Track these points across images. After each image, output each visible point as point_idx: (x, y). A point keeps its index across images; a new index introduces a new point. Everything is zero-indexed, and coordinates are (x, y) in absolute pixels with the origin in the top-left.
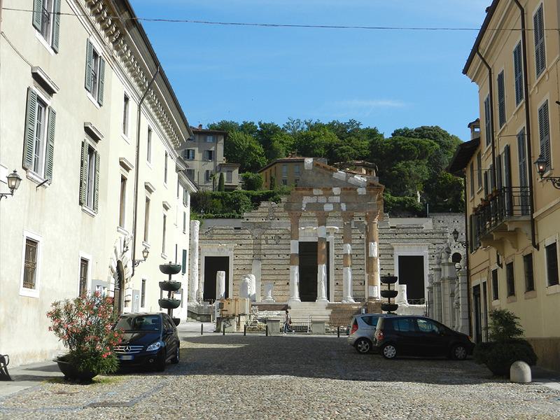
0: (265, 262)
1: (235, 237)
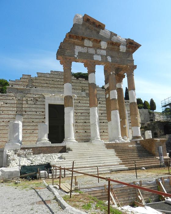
0: (25, 116)
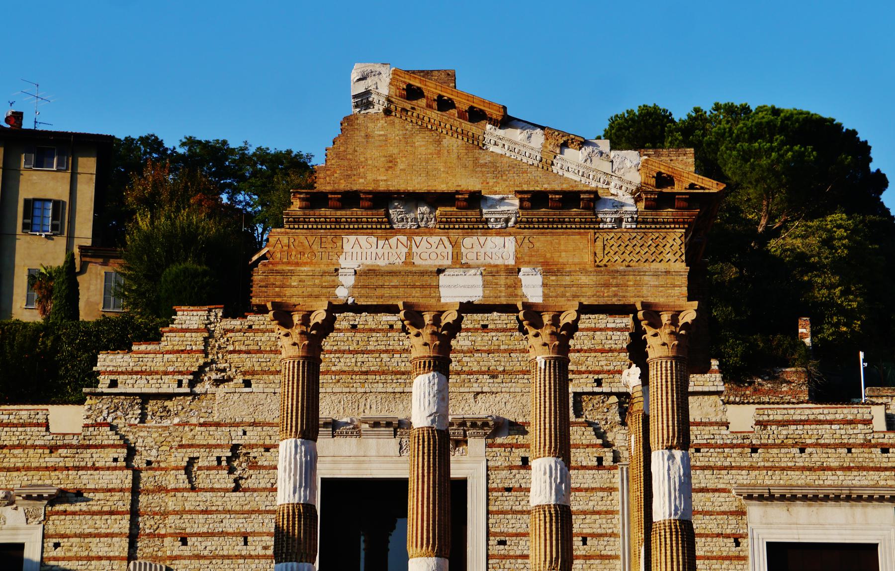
1: (52, 460)
